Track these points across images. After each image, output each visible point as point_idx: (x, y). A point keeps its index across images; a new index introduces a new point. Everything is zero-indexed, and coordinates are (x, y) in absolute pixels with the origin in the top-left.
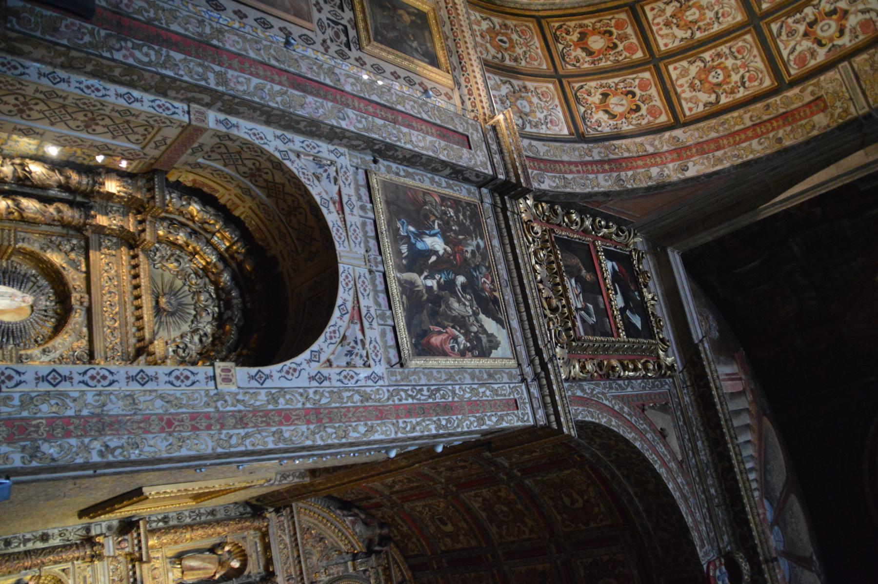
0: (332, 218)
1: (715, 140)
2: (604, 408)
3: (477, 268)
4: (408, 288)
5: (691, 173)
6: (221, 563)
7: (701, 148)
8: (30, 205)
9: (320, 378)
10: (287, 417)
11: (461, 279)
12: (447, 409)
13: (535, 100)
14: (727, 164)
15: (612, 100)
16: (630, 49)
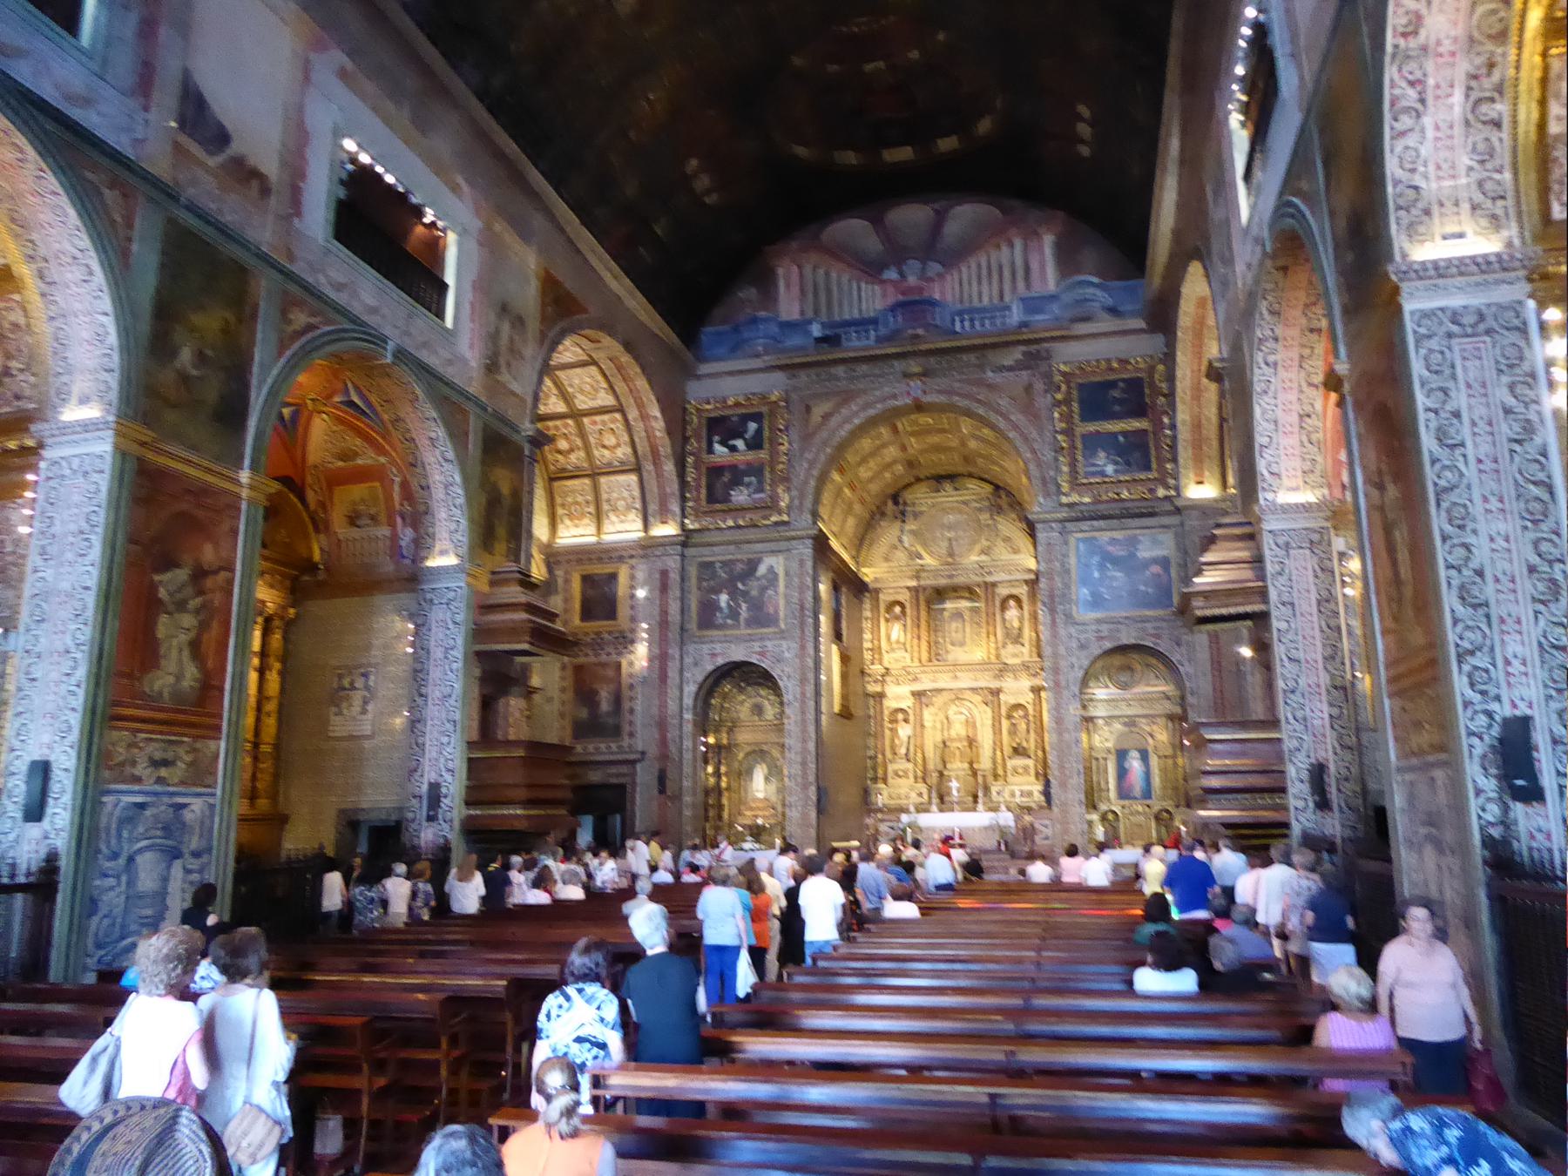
0: (720, 661)
1: (635, 399)
2: (806, 482)
3: (732, 570)
4: (749, 624)
5: (658, 414)
6: (897, 618)
7: (640, 406)
8: (723, 769)
9: (789, 677)
10: (803, 694)
11: (740, 586)
12: (802, 608)
13: (615, 495)
14: (653, 398)
15: (607, 443)
16: (566, 426)
